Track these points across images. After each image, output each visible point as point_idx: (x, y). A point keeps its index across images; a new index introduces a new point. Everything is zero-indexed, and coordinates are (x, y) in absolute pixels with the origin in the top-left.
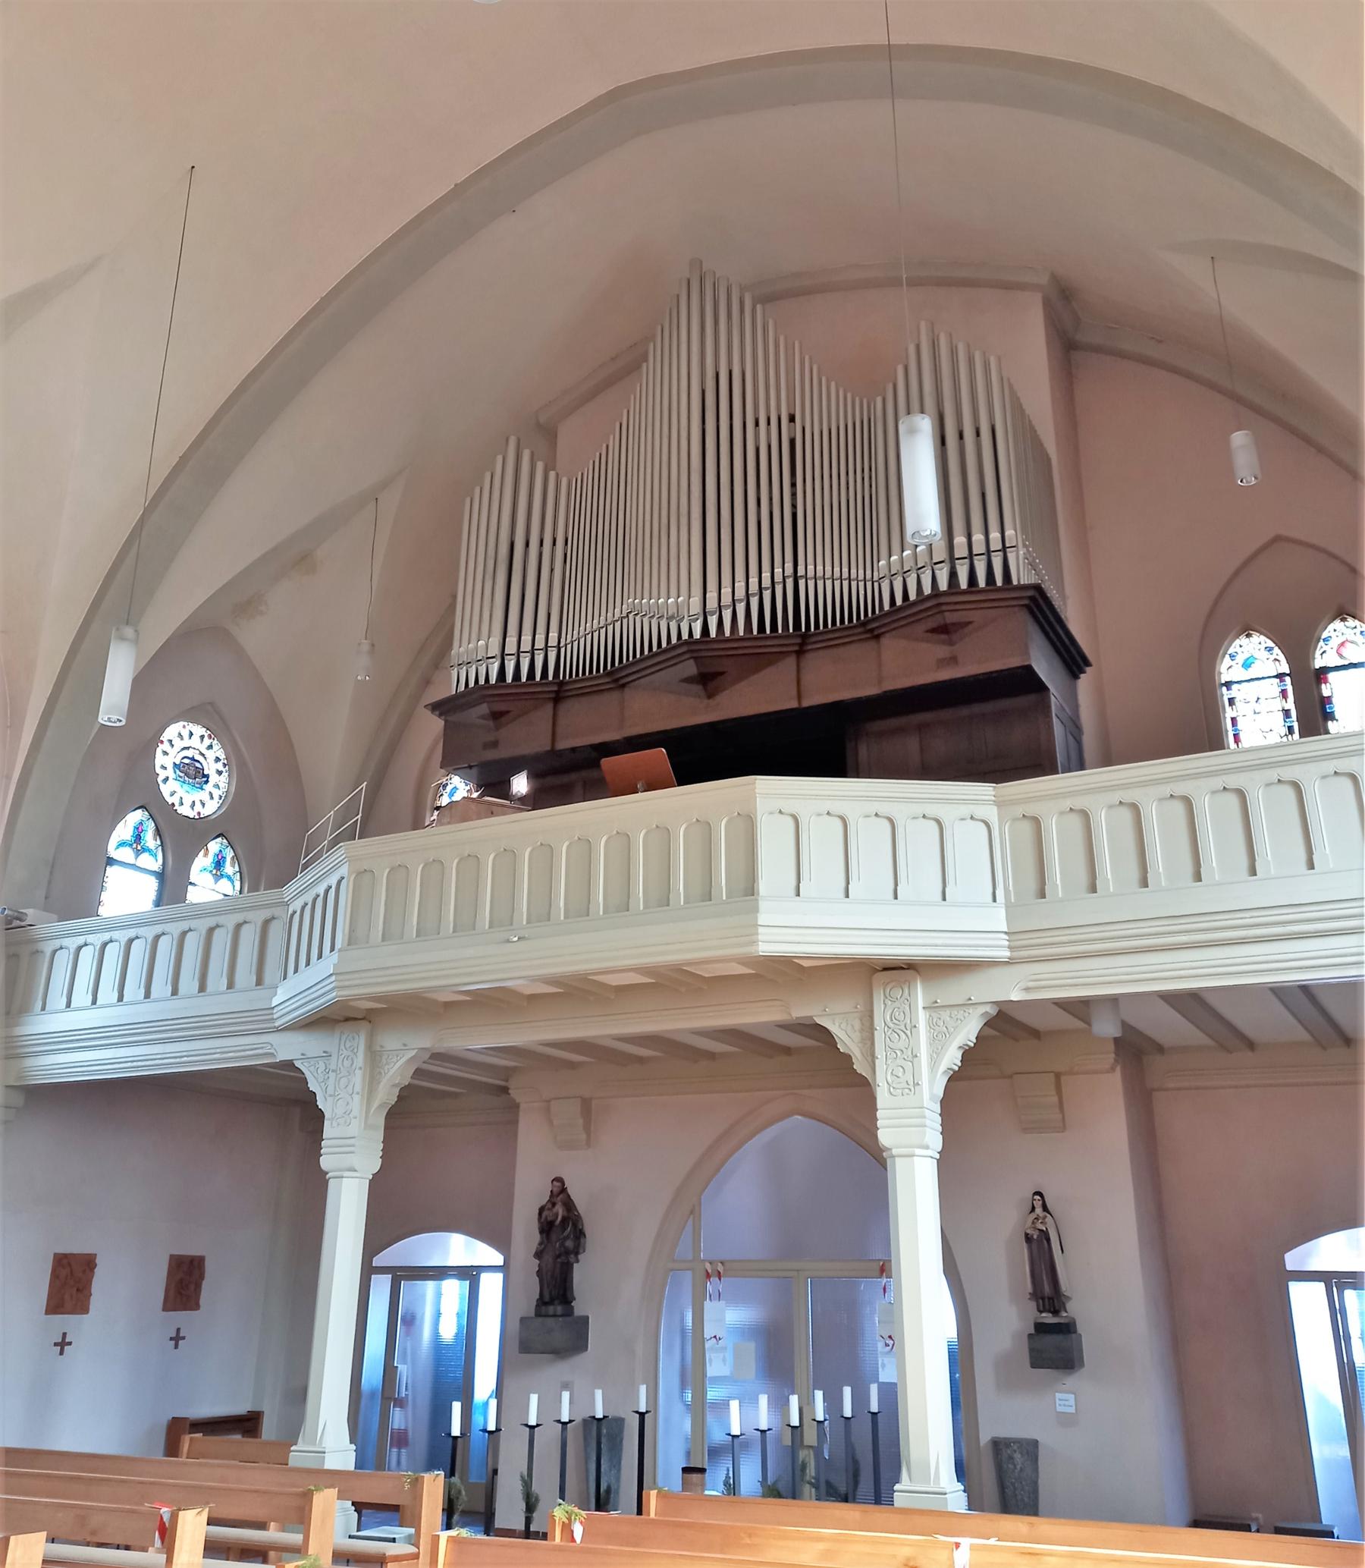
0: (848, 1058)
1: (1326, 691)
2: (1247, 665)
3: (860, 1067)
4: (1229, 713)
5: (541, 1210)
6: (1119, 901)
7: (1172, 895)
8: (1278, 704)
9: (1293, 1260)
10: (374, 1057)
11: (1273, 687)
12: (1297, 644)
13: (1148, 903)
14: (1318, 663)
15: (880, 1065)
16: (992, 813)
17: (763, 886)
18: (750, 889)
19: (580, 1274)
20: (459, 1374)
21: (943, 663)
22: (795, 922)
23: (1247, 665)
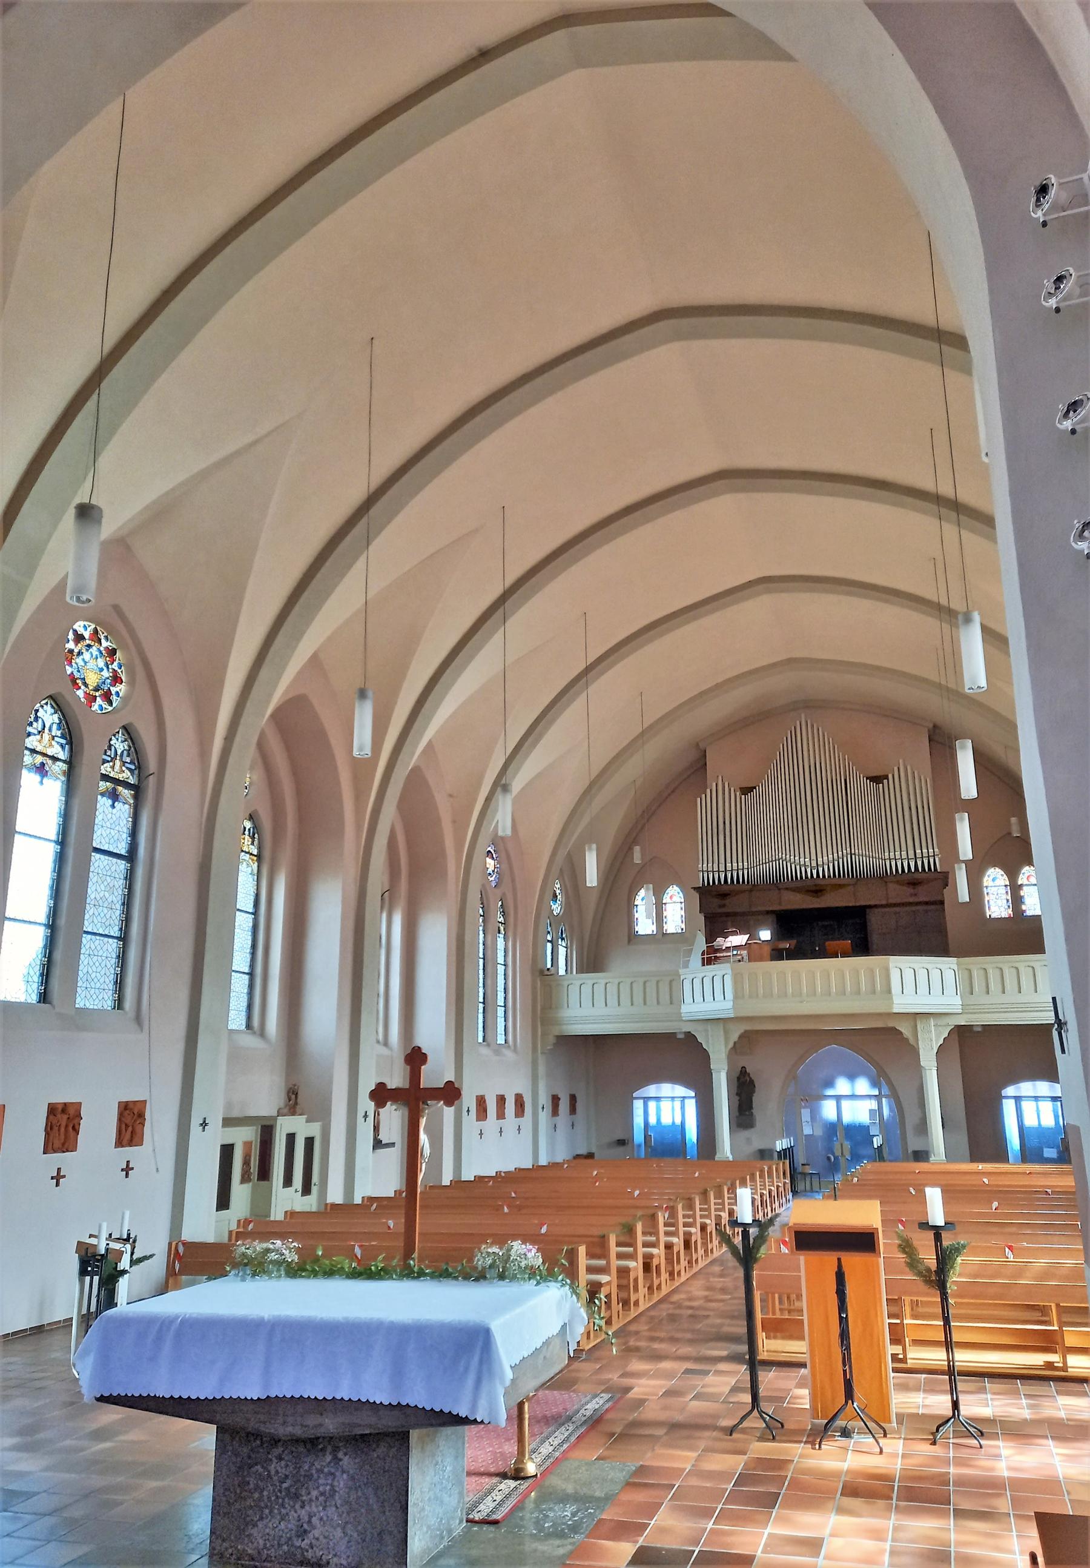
0: (907, 1040)
1: (1022, 893)
2: (994, 880)
3: (912, 1041)
4: (987, 898)
5: (738, 1078)
6: (995, 997)
7: (1011, 997)
8: (1004, 897)
9: (1010, 1091)
10: (726, 1032)
11: (1003, 890)
12: (1012, 874)
13: (1005, 999)
14: (1020, 883)
15: (920, 1043)
16: (955, 967)
17: (893, 991)
18: (889, 991)
19: (756, 1099)
20: (679, 1136)
21: (911, 895)
22: (903, 1001)
23: (994, 880)
